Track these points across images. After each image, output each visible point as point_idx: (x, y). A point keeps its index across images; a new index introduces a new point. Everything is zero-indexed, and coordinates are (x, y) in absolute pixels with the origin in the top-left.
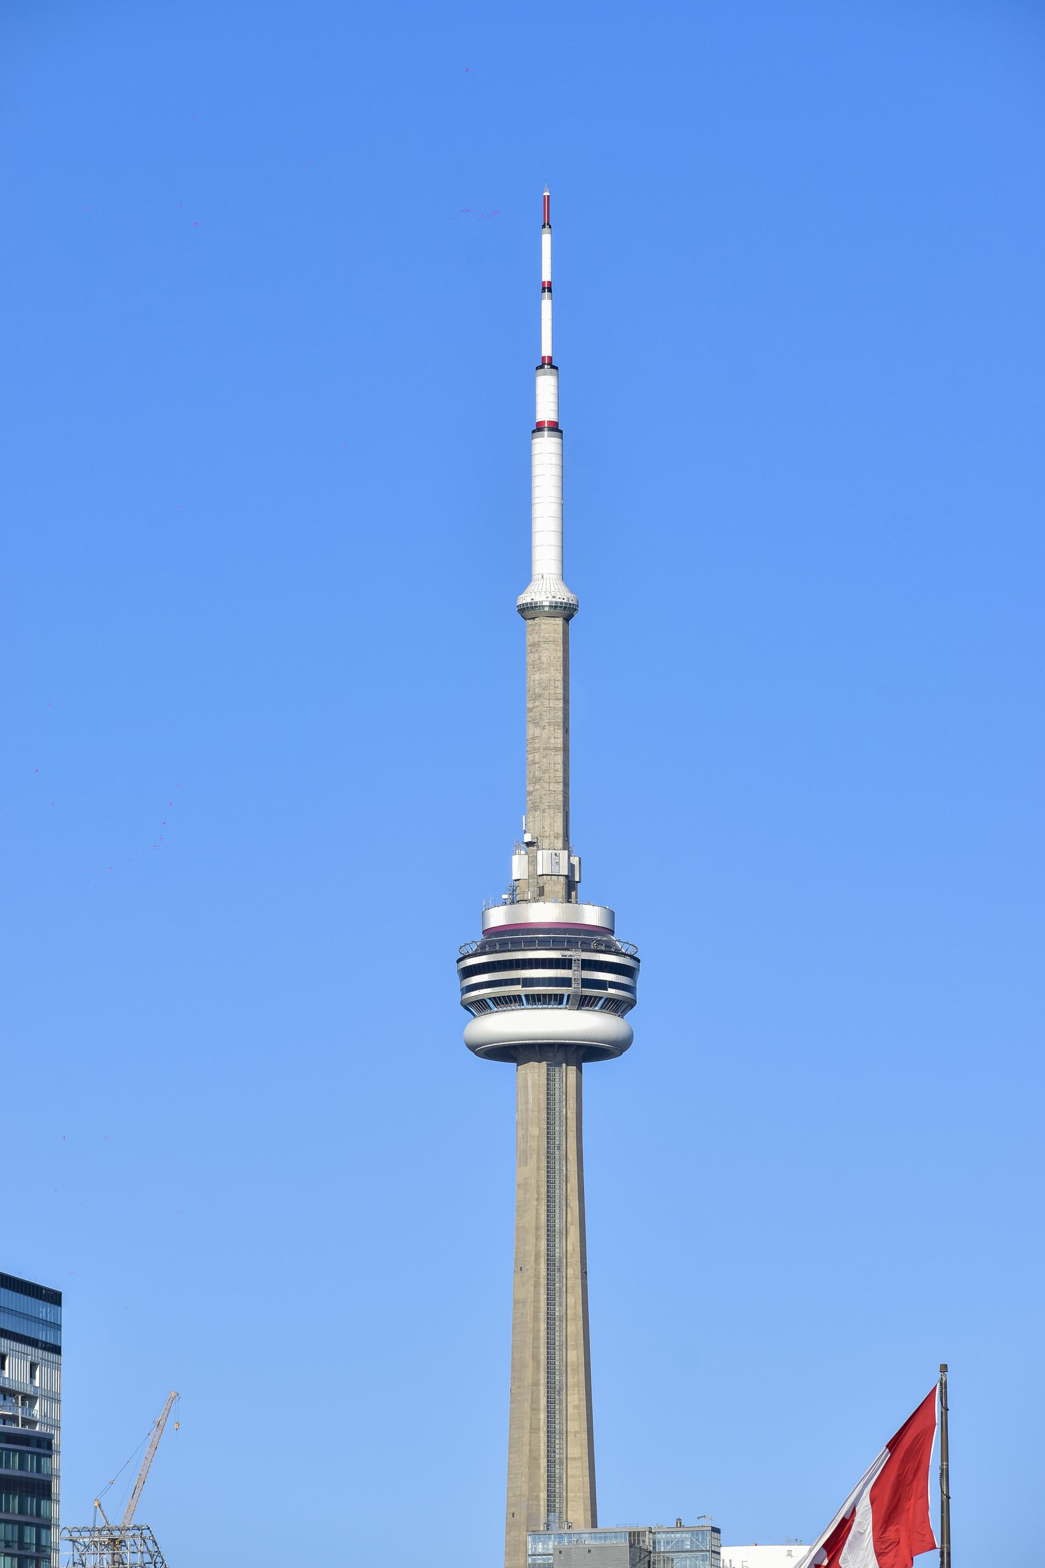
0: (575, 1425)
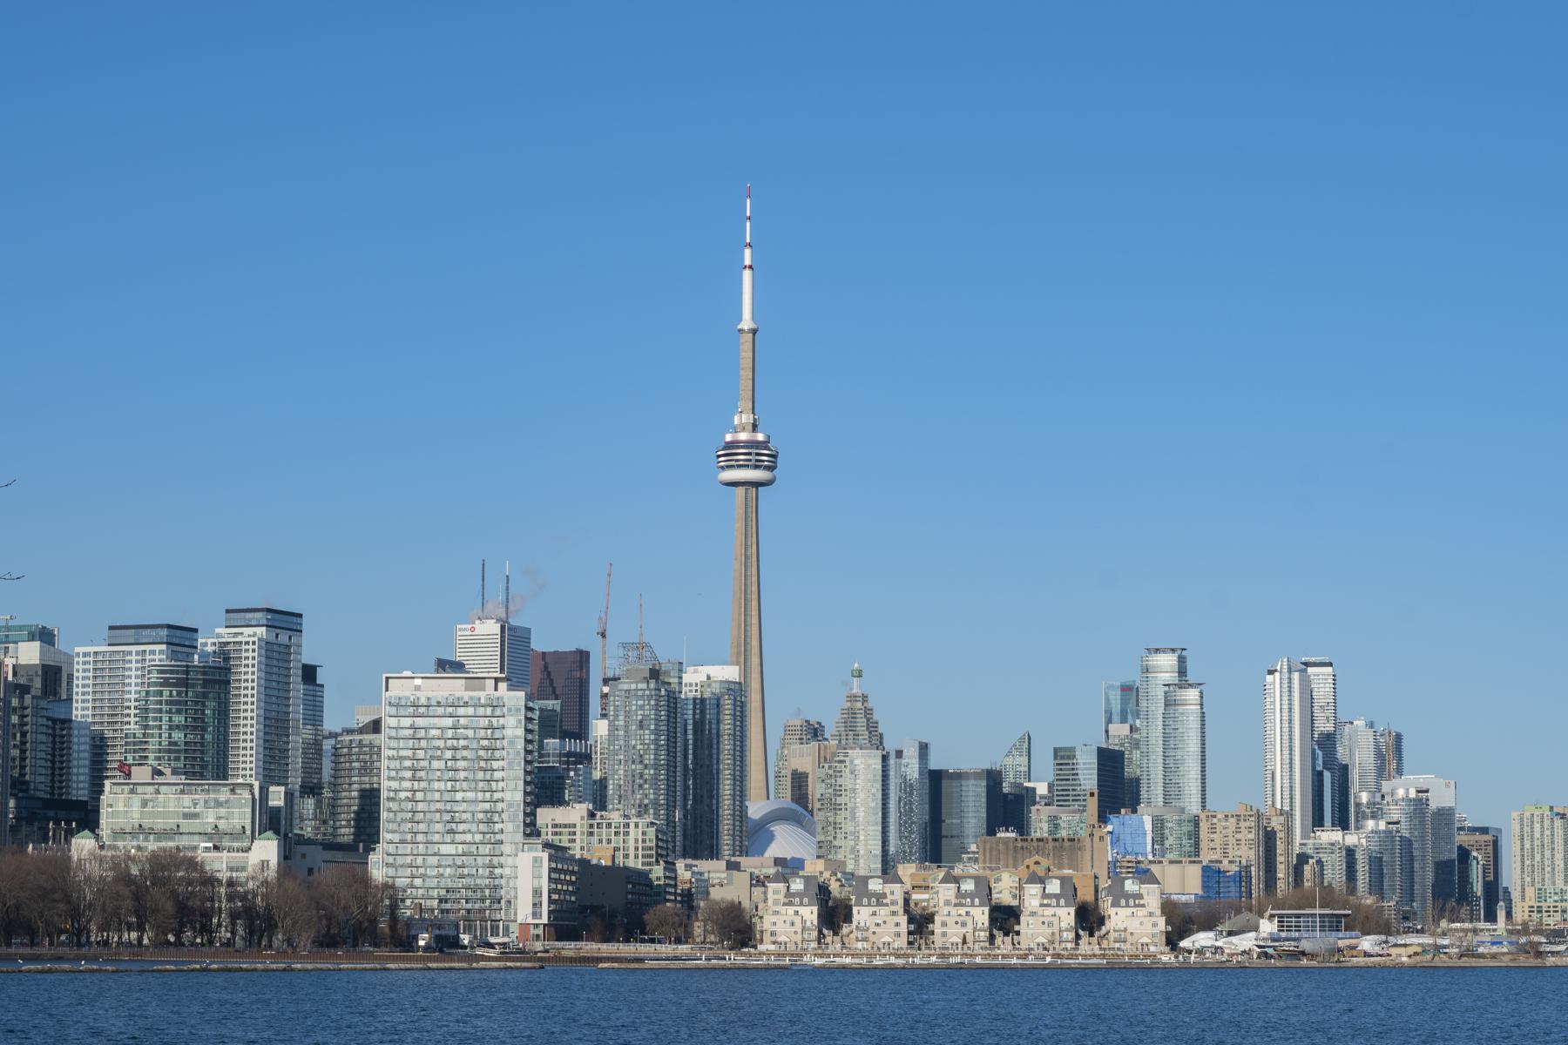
0: (755, 613)
